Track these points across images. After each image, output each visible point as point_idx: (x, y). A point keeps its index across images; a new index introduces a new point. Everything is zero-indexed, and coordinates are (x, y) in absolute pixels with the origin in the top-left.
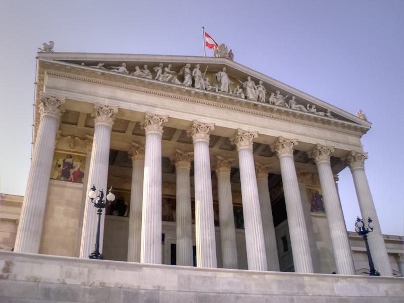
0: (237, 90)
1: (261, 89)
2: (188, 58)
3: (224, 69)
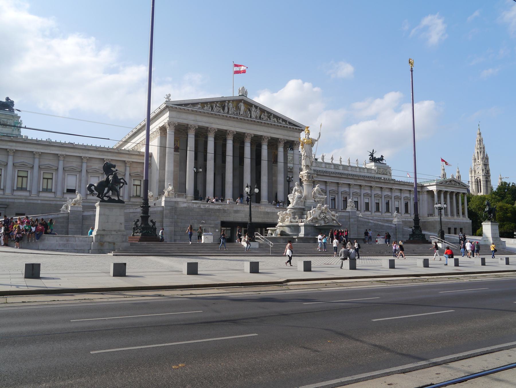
0: (247, 112)
1: (258, 111)
2: (227, 98)
3: (243, 101)
